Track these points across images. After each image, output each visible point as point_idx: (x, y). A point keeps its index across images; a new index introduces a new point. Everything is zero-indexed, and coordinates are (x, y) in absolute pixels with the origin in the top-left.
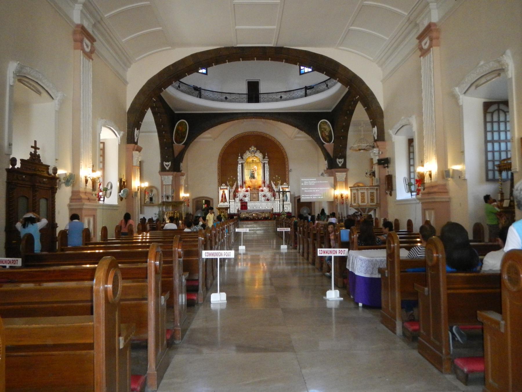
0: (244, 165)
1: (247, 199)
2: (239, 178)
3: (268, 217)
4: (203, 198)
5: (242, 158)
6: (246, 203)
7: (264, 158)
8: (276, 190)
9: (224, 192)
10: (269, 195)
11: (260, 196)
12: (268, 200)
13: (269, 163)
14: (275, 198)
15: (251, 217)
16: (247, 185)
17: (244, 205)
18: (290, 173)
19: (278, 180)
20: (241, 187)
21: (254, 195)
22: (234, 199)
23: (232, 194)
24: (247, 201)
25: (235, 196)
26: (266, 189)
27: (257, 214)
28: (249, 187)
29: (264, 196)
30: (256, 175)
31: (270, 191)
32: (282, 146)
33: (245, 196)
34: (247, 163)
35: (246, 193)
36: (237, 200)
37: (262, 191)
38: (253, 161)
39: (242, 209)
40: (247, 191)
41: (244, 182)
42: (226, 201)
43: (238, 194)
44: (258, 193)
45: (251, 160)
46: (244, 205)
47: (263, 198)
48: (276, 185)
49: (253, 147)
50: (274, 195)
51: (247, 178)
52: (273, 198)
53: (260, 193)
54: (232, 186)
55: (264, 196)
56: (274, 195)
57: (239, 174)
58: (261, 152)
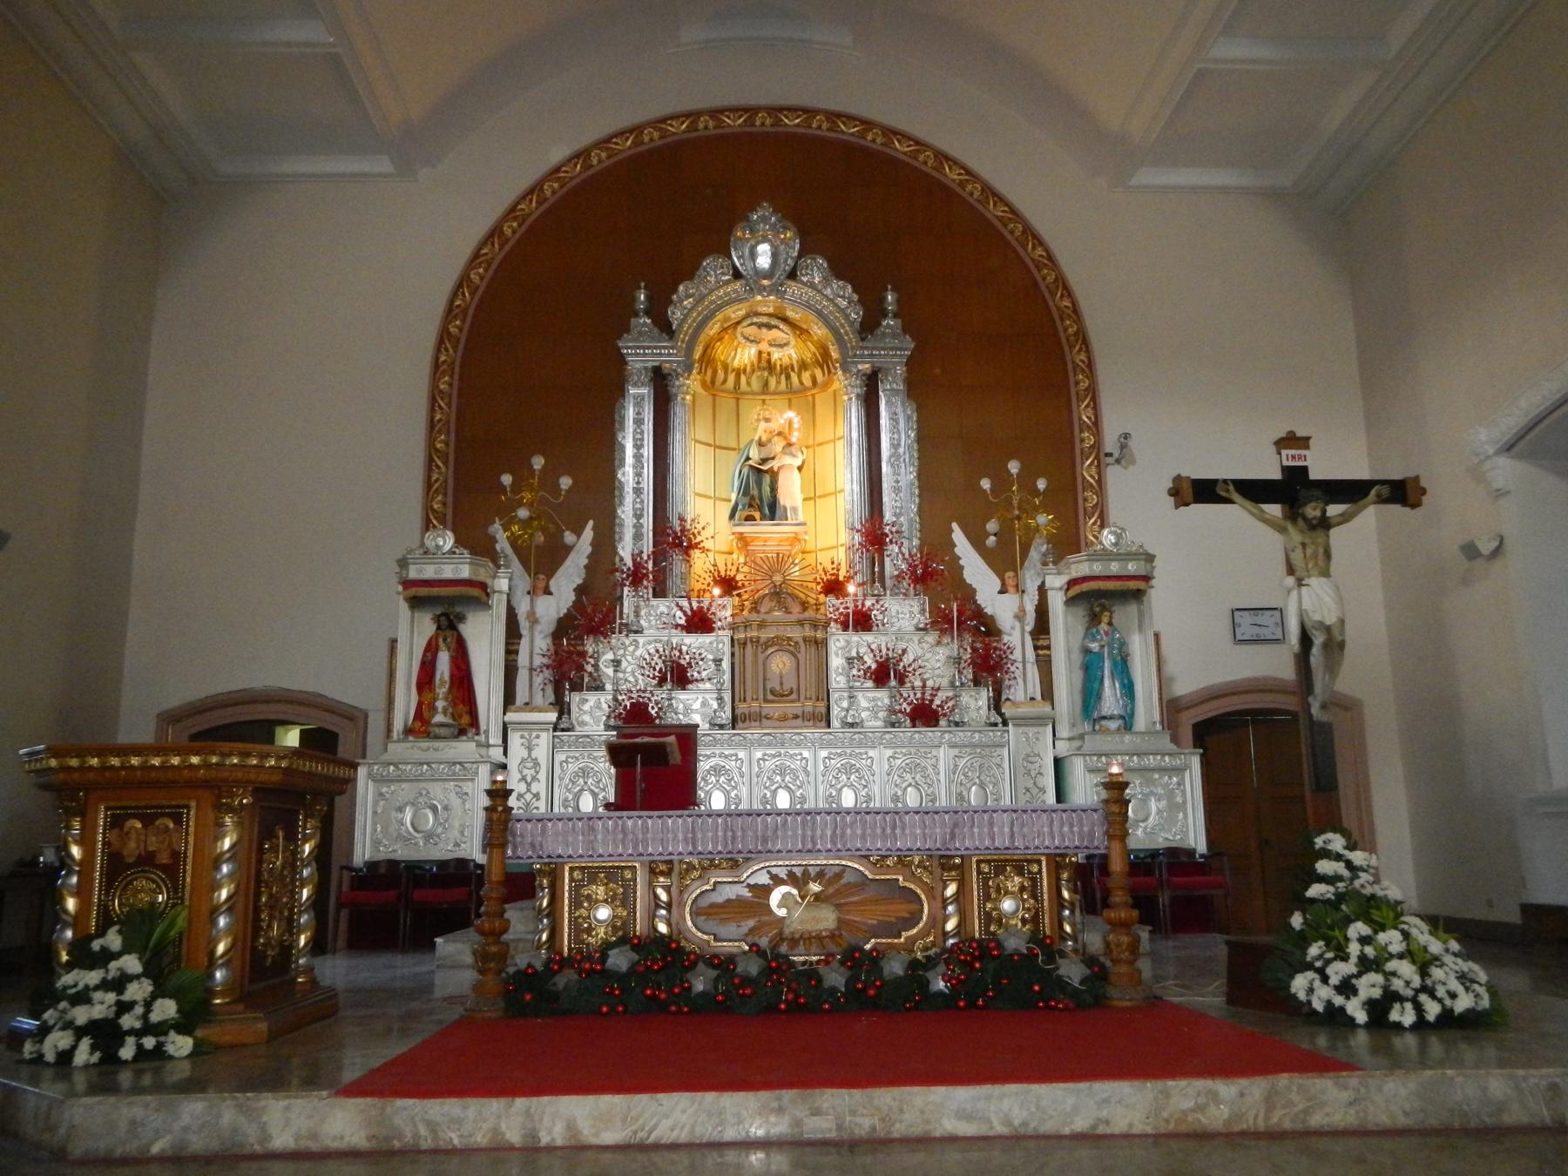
0: (690, 387)
1: (694, 707)
2: (626, 513)
3: (1046, 946)
4: (293, 704)
5: (665, 328)
6: (687, 737)
7: (868, 327)
8: (1004, 609)
9: (449, 625)
10: (935, 662)
11: (837, 681)
12: (924, 715)
13: (917, 389)
14: (996, 704)
15: (731, 940)
16: (701, 564)
17: (654, 767)
18: (1113, 474)
19: (1029, 510)
20: (637, 577)
21: (780, 664)
22: (562, 708)
23: (537, 646)
24: (696, 718)
25: (568, 673)
26: (903, 615)
27: (836, 889)
28: (728, 585)
29: (883, 674)
30: (791, 490)
31: (940, 622)
32: (1030, 233)
33: (678, 675)
34: (711, 386)
35: (693, 642)
36: (593, 713)
37: (862, 621)
38: (766, 365)
39: (625, 801)
40: (699, 622)
41: (673, 540)
42: (466, 719)
43: (604, 655)
44: (821, 645)
45: (745, 355)
46: (654, 767)
47: (872, 702)
48: (1005, 561)
49: (763, 214)
50: (987, 666)
51: (705, 494)
52: (976, 702)
53: (841, 645)
54: (543, 562)
55: (883, 674)
56: (987, 666)
57: (627, 475)
58: (840, 269)
